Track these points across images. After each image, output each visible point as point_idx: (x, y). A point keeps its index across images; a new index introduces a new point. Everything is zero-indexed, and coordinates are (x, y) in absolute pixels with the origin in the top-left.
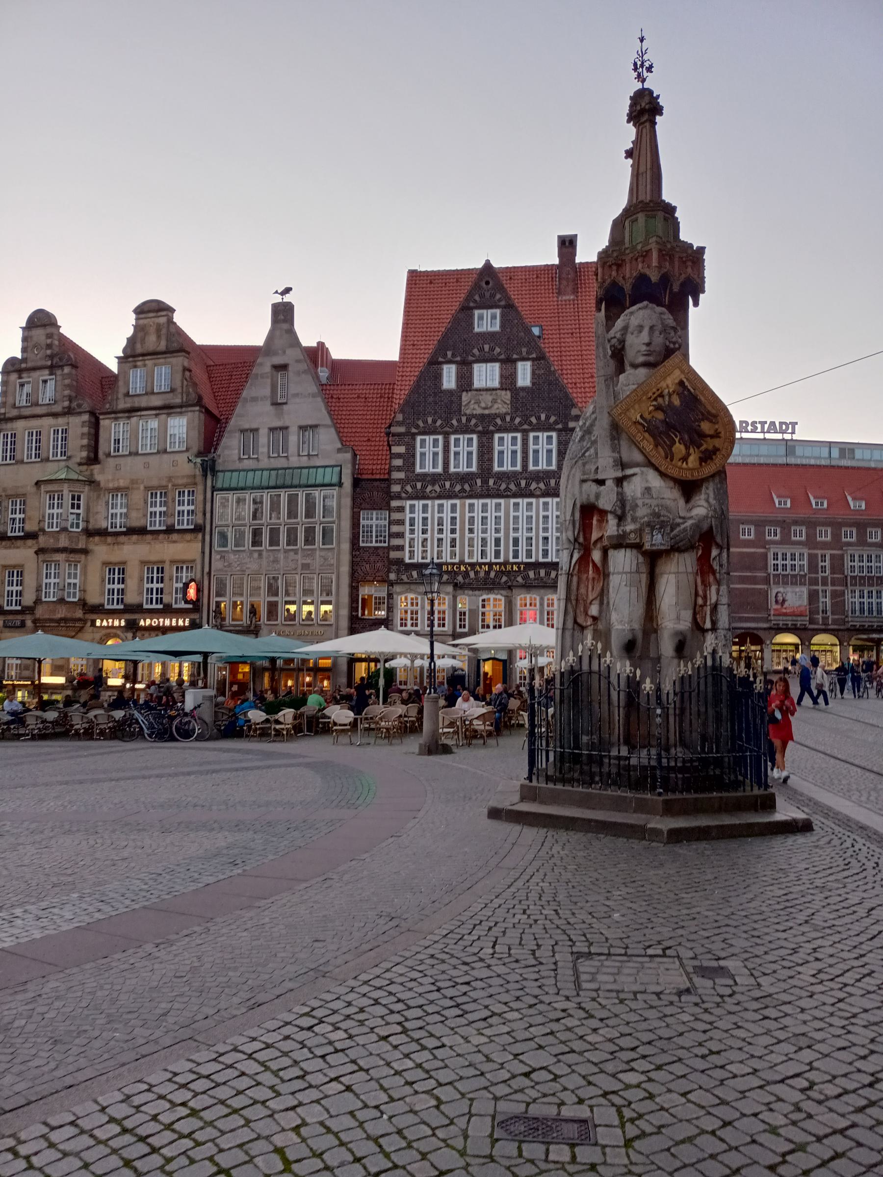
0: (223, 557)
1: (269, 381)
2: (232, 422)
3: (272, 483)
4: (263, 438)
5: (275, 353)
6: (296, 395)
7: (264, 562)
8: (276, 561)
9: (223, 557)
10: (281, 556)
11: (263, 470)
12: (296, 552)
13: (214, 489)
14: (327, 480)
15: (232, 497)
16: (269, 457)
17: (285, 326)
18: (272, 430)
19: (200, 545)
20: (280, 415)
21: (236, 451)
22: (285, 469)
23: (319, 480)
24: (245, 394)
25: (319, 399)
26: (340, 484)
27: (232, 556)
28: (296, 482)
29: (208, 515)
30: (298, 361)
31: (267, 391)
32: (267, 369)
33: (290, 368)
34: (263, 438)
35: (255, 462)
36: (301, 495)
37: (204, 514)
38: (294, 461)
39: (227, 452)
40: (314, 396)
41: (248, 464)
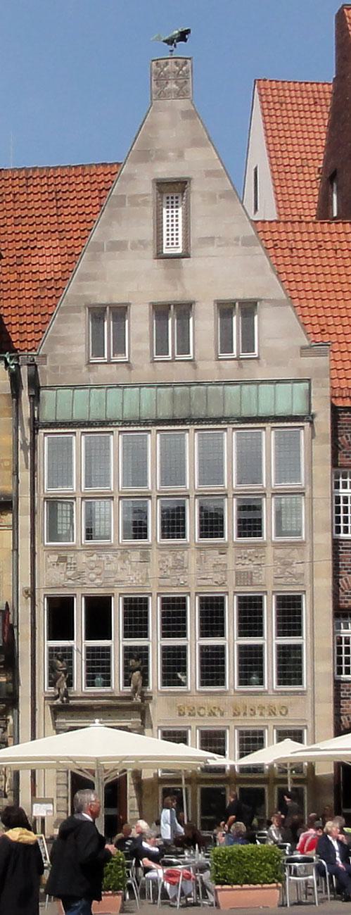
0: (63, 559)
1: (149, 211)
2: (72, 289)
3: (164, 413)
4: (139, 325)
5: (161, 158)
6: (210, 240)
7: (154, 569)
8: (180, 566)
9: (63, 559)
10: (191, 558)
11: (141, 386)
12: (223, 550)
13: (35, 425)
14: (282, 410)
15: (79, 441)
16: (153, 362)
17: (182, 104)
18: (160, 311)
19: (9, 534)
20: (175, 278)
21: (82, 349)
22: (189, 385)
23: (265, 409)
24: (95, 236)
25: (259, 250)
26: (309, 418)
27: (83, 558)
28: (214, 412)
29: (25, 476)
30: (210, 174)
31: (148, 231)
32: (146, 188)
33: (194, 187)
34: (139, 325)
35: (124, 368)
36: (230, 440)
37: (16, 473)
38: (209, 369)
39: (60, 350)
40: (246, 242)
41: (105, 373)
